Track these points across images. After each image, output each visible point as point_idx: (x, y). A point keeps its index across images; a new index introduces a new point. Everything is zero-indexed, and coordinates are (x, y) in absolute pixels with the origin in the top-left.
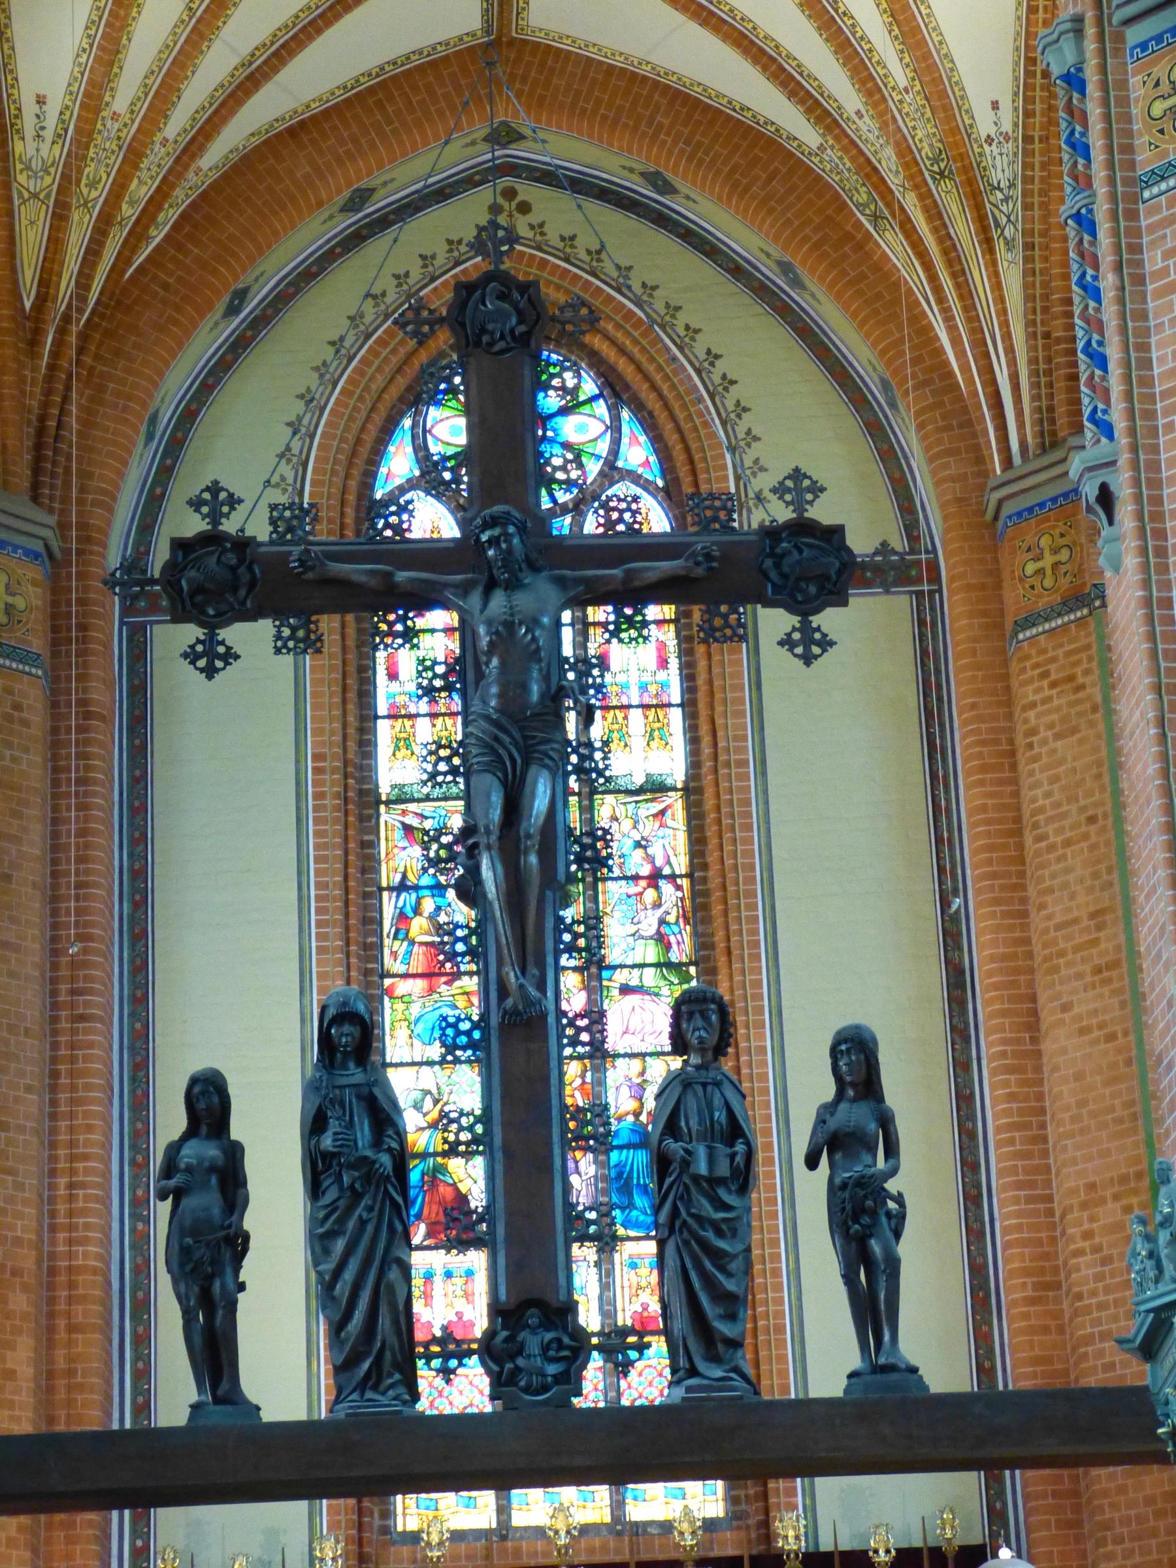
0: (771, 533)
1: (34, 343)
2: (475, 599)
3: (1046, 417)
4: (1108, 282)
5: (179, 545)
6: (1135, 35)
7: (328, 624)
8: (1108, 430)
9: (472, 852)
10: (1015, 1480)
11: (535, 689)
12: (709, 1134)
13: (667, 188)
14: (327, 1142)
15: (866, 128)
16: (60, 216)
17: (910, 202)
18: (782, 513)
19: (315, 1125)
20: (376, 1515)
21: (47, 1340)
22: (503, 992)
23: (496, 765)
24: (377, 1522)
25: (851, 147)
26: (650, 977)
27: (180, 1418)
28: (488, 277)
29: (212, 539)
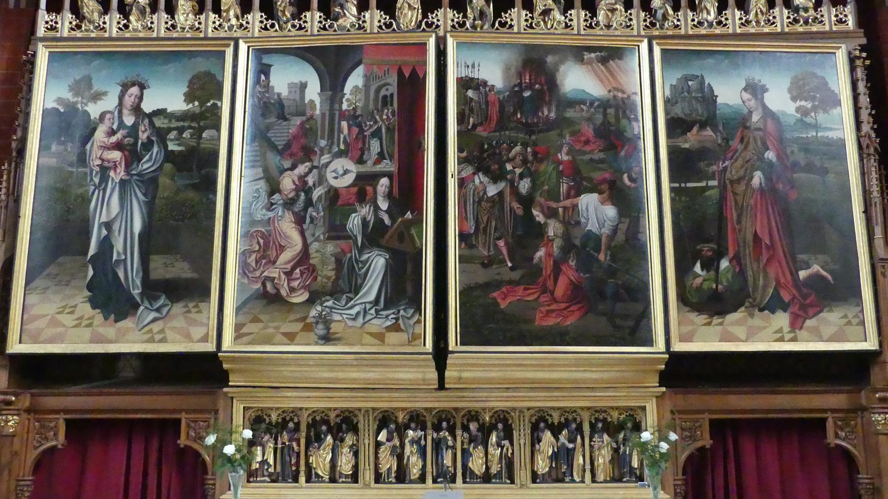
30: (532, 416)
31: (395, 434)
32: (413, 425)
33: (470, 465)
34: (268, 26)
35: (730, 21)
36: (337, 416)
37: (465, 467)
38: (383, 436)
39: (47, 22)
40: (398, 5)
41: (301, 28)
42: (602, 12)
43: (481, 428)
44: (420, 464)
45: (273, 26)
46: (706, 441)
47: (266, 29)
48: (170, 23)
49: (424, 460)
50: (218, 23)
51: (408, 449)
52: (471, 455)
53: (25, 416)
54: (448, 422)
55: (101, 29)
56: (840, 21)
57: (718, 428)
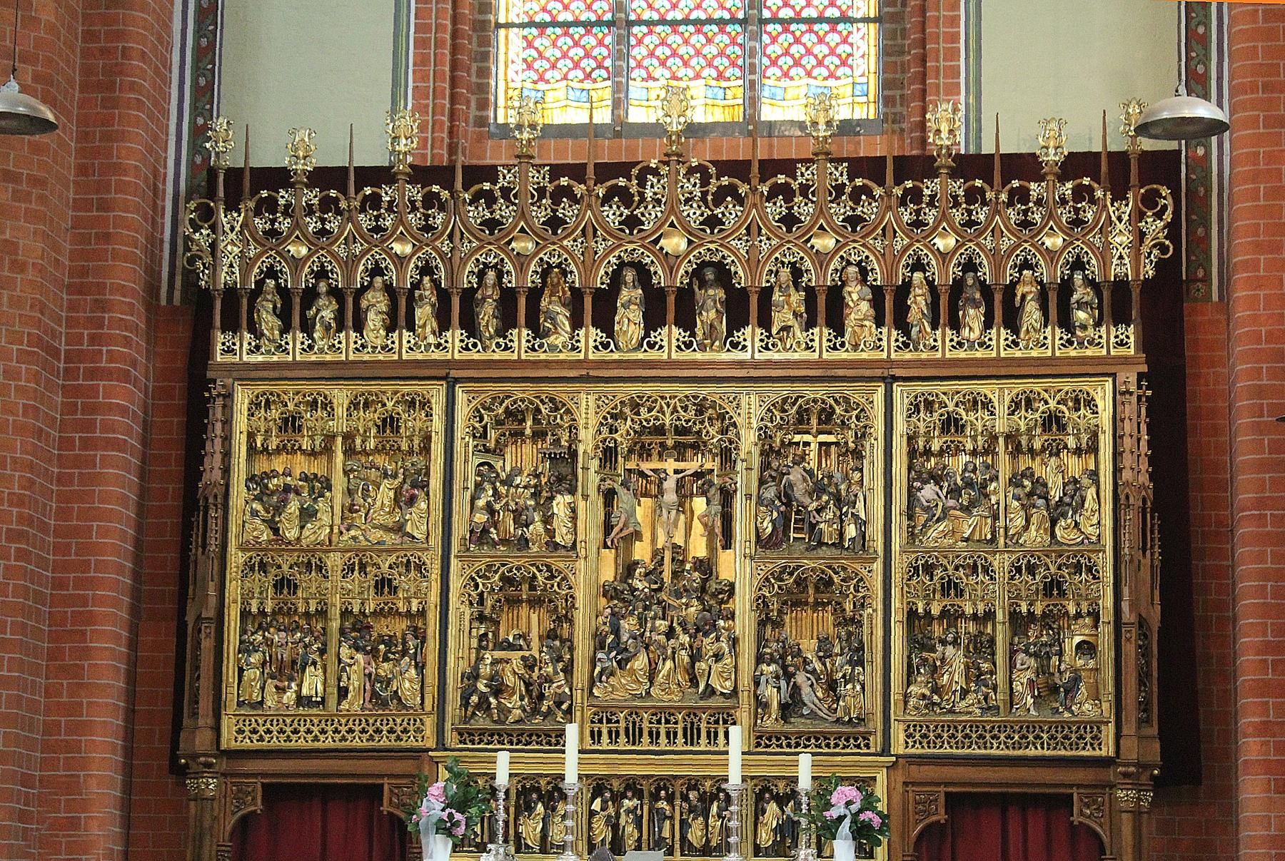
20: (473, 104)
24: (473, 112)
30: (756, 785)
31: (610, 803)
32: (629, 794)
33: (689, 836)
34: (470, 346)
35: (994, 343)
36: (549, 783)
37: (683, 838)
38: (597, 805)
39: (223, 344)
40: (617, 318)
41: (506, 348)
42: (850, 329)
43: (702, 798)
44: (636, 835)
45: (475, 345)
46: (941, 816)
47: (467, 349)
48: (359, 342)
49: (641, 831)
50: (413, 341)
51: (622, 821)
52: (690, 826)
53: (222, 779)
54: (666, 789)
55: (283, 351)
56: (1122, 344)
57: (954, 802)
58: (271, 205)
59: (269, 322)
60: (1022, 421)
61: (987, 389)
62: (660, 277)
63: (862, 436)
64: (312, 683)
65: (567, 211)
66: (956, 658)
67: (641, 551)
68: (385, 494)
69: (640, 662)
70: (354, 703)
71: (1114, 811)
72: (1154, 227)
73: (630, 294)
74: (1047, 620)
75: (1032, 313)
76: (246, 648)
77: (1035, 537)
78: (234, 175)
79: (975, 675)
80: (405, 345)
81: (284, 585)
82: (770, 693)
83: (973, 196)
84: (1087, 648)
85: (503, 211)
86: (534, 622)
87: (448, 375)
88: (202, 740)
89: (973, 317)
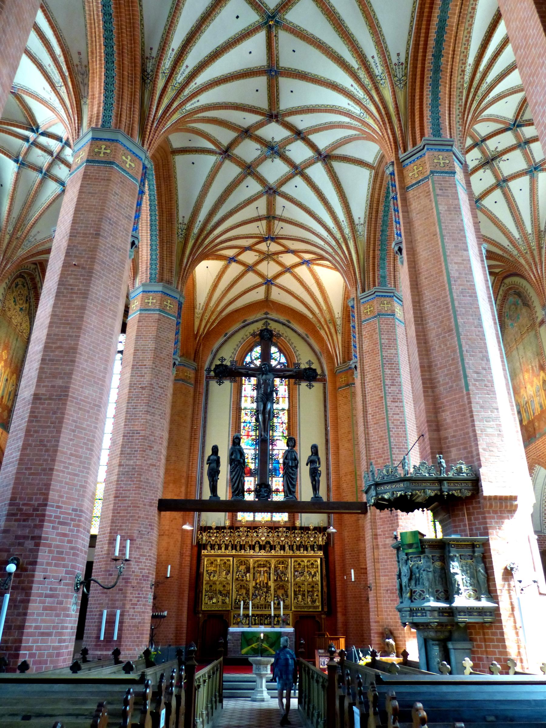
0: (305, 369)
1: (196, 338)
2: (260, 376)
3: (344, 358)
4: (357, 336)
5: (216, 365)
6: (362, 301)
7: (237, 378)
8: (356, 357)
9: (258, 414)
10: (332, 516)
11: (269, 390)
12: (292, 459)
13: (289, 322)
14: (233, 457)
15: (319, 315)
16: (201, 321)
17: (325, 327)
18: (307, 366)
19: (231, 454)
21: (187, 487)
22: (261, 436)
23: (262, 401)
25: (317, 318)
26: (281, 438)
27: (208, 498)
28: (265, 329)
29: (221, 365)
58: (209, 532)
59: (209, 548)
60: (309, 564)
61: (304, 559)
62: (261, 543)
63: (288, 565)
64: (214, 600)
65: (249, 534)
66: (300, 597)
67: (258, 581)
68: (224, 572)
69: (259, 597)
70: (220, 603)
71: (321, 618)
72: (325, 538)
73: (257, 545)
74: (312, 591)
75: (309, 549)
76: (206, 595)
77: (310, 580)
78: (205, 527)
79: (303, 599)
80: (227, 552)
81: (211, 586)
82: (276, 602)
83: (302, 533)
84: (317, 595)
85: (241, 534)
86: (244, 591)
87: (233, 556)
88: (200, 609)
89: (302, 549)
